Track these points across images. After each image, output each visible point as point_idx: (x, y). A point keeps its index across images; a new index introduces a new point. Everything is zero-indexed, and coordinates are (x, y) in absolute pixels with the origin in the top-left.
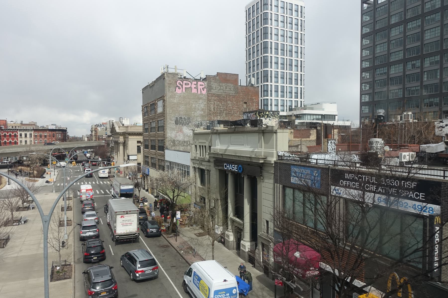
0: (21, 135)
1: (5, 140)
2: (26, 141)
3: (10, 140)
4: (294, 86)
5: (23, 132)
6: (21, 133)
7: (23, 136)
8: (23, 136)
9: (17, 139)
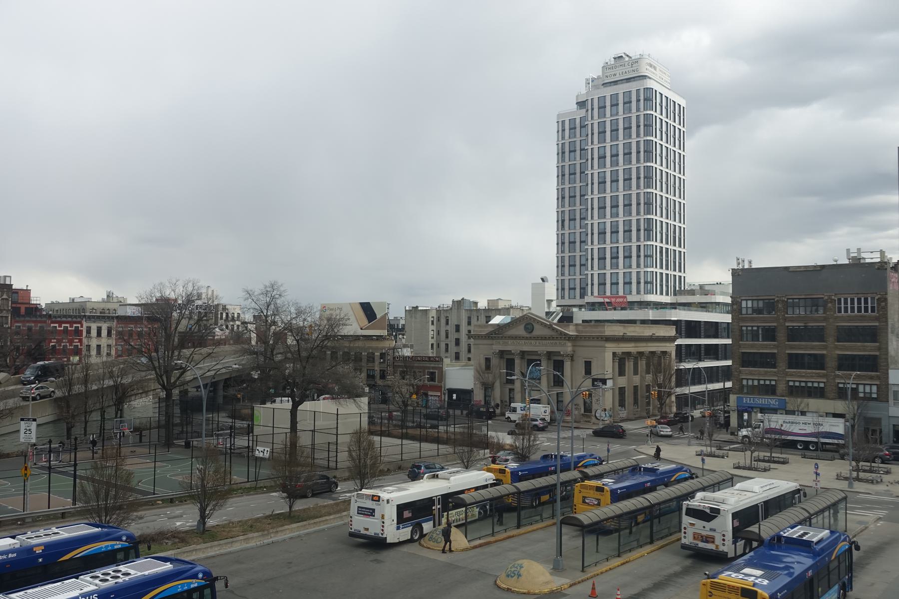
0: (89, 330)
1: (65, 343)
2: (99, 347)
3: (65, 343)
4: (634, 245)
5: (94, 322)
6: (89, 325)
7: (94, 333)
8: (94, 333)
9: (81, 341)
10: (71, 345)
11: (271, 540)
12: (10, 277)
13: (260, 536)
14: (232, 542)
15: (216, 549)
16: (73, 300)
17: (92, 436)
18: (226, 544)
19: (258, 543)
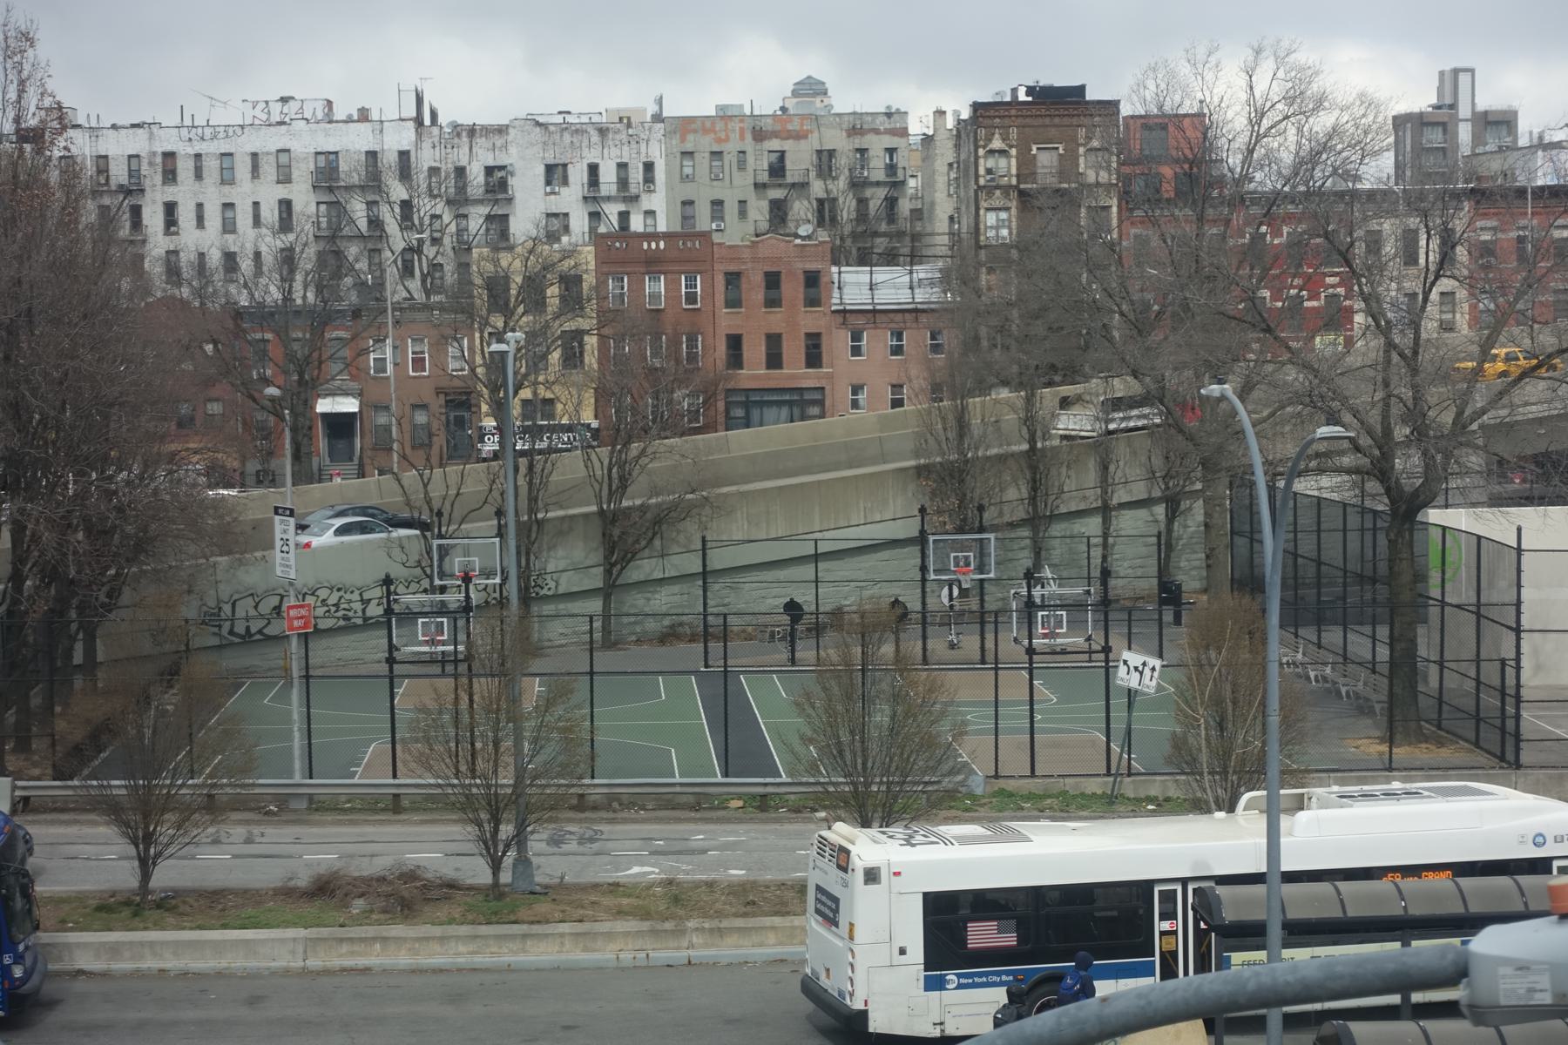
10: (1314, 296)
11: (685, 953)
12: (1472, 71)
13: (639, 934)
14: (525, 936)
15: (462, 948)
16: (1541, 138)
17: (945, 591)
18: (498, 937)
19: (626, 957)
